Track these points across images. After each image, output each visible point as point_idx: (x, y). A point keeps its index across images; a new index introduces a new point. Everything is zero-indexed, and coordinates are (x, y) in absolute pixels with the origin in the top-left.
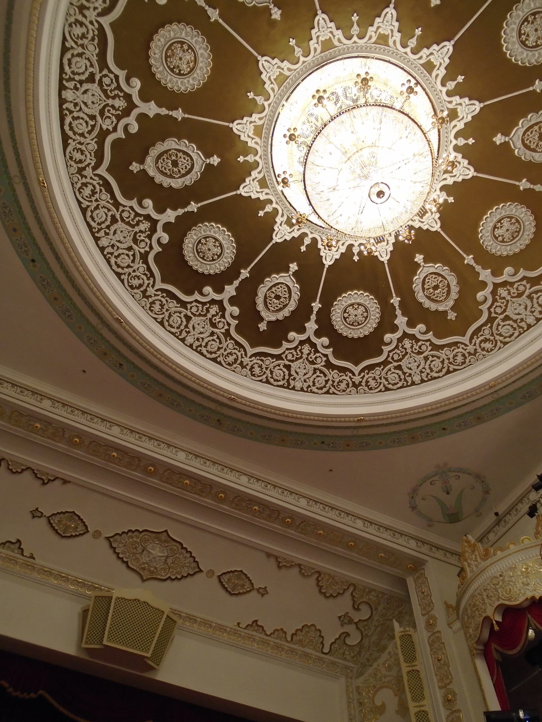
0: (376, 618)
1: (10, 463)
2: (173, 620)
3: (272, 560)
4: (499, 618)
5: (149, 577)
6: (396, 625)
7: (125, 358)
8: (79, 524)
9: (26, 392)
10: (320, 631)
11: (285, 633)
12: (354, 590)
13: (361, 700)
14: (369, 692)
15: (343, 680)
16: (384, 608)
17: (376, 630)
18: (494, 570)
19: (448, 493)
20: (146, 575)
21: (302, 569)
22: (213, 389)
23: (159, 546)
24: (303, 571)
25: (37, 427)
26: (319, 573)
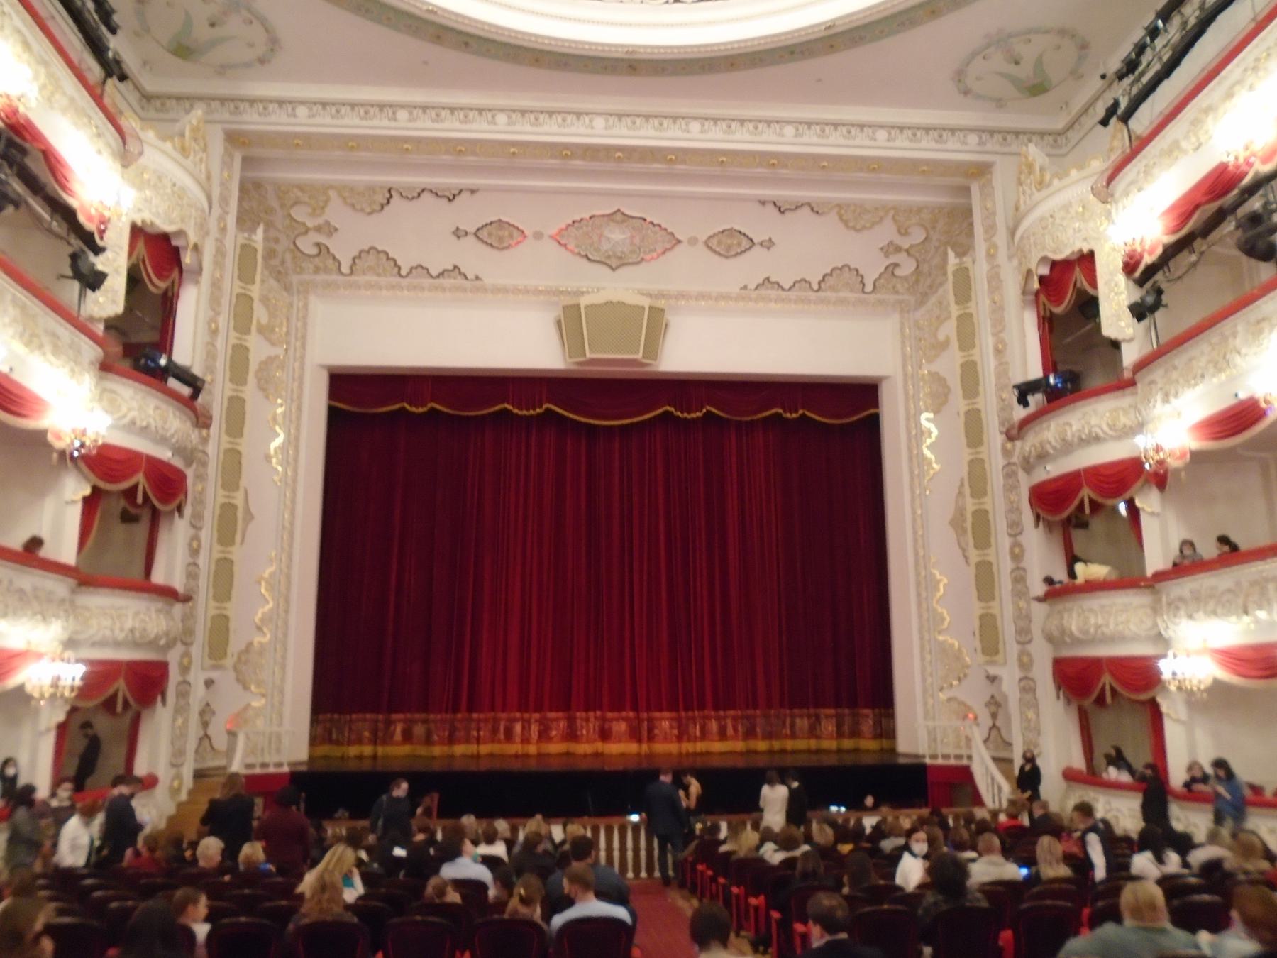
3: (770, 207)
4: (1045, 271)
6: (951, 254)
15: (896, 317)
18: (1043, 209)
19: (1017, 63)
20: (614, 262)
26: (839, 206)
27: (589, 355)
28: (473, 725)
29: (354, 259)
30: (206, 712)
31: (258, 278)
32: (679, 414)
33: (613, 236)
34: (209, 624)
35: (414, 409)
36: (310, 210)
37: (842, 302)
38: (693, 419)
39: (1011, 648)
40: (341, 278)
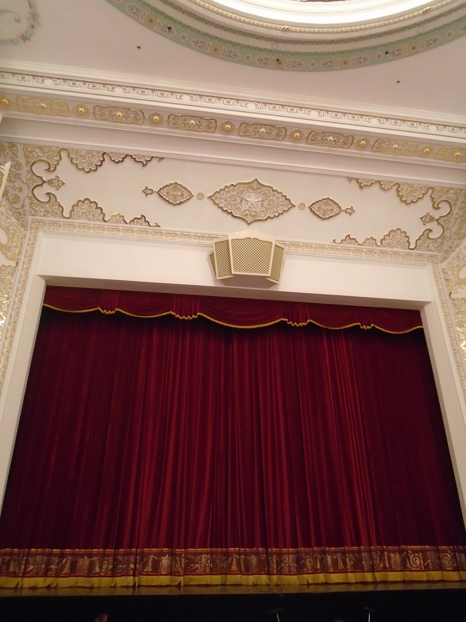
0: (455, 211)
1: (111, 155)
2: (280, 248)
3: (354, 183)
5: (253, 220)
7: (171, 18)
8: (183, 191)
9: (98, 86)
10: (405, 232)
11: (375, 240)
12: (433, 192)
13: (447, 278)
14: (454, 270)
15: (430, 266)
16: (462, 202)
17: (456, 222)
20: (249, 220)
21: (382, 185)
22: (265, 24)
23: (254, 193)
24: (383, 186)
25: (119, 116)
26: (398, 185)
27: (233, 272)
28: (132, 558)
29: (74, 206)
36: (47, 168)
37: (396, 253)
40: (63, 220)
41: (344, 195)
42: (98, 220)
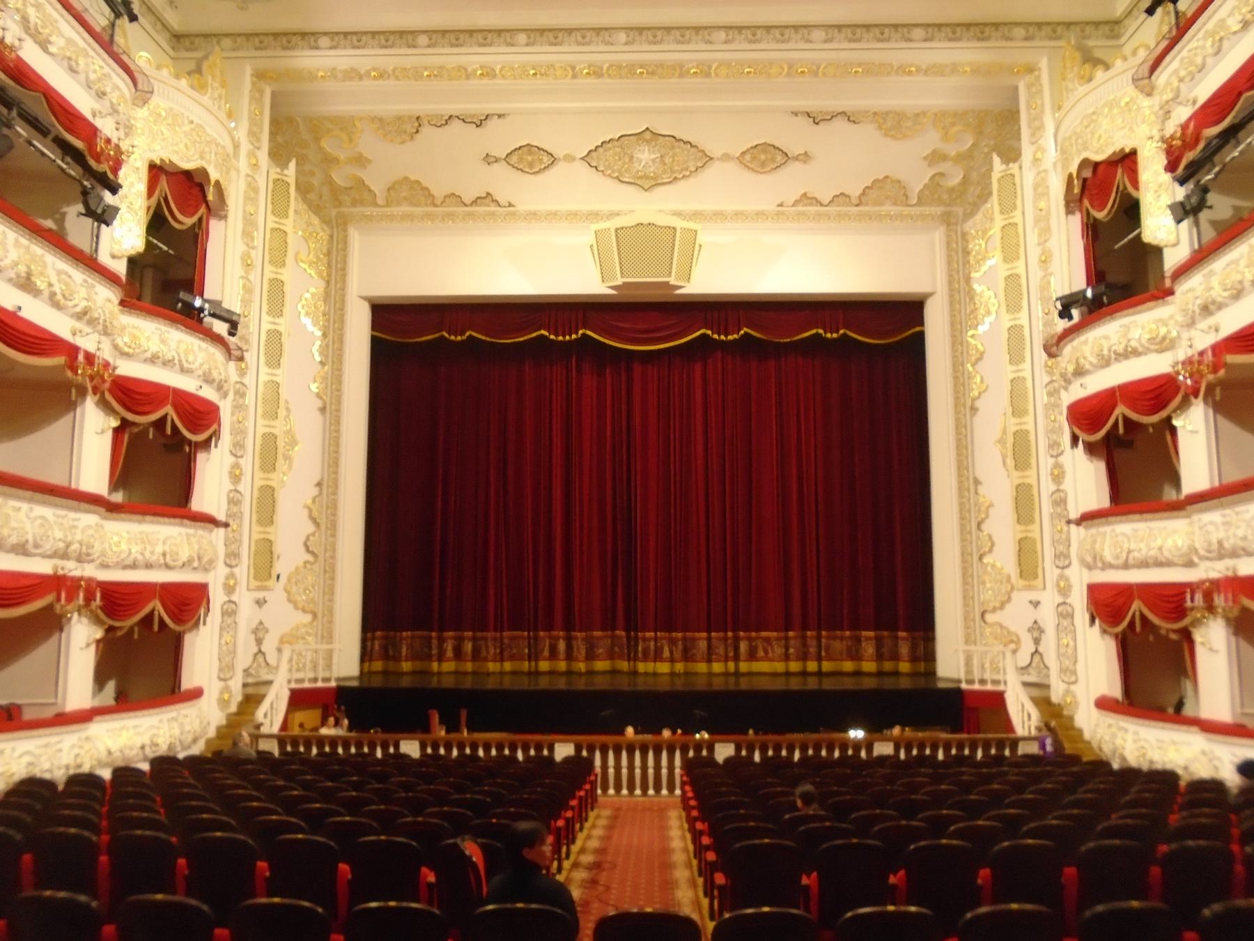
11: (849, 197)
15: (943, 229)
20: (648, 183)
27: (619, 281)
30: (259, 632)
31: (291, 212)
32: (716, 336)
33: (640, 156)
34: (253, 548)
35: (453, 338)
38: (730, 341)
39: (1051, 572)
41: (794, 136)
42: (426, 205)
